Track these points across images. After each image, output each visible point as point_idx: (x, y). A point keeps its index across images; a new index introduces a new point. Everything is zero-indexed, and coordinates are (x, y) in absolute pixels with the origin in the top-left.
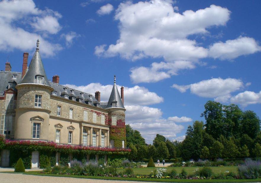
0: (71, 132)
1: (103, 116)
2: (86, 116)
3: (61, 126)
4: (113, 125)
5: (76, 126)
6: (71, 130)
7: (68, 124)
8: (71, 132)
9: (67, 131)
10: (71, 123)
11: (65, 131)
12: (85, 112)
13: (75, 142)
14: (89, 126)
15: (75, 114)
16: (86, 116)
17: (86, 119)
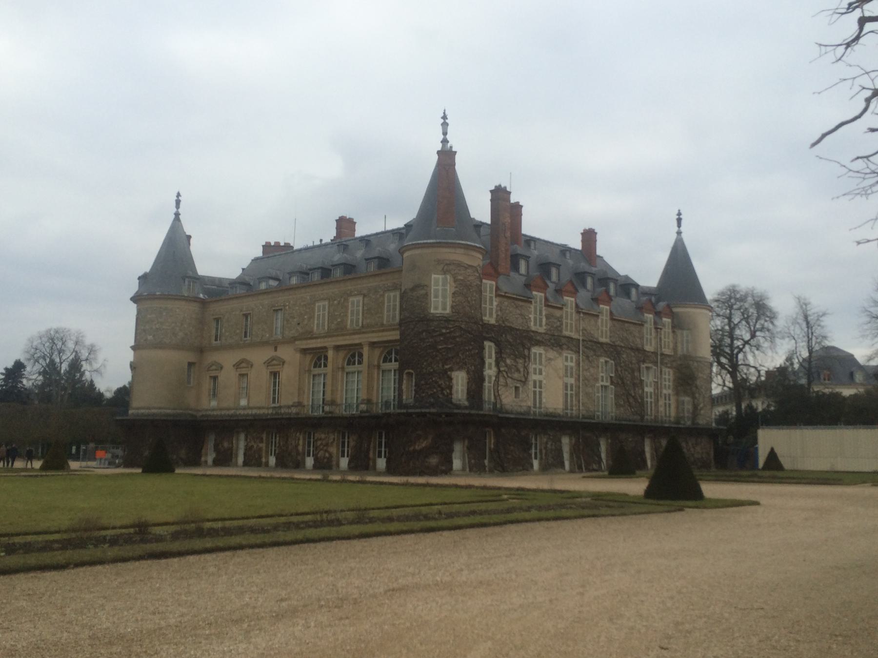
0: (275, 374)
1: (392, 294)
2: (324, 315)
3: (250, 365)
4: (432, 311)
5: (287, 353)
6: (276, 369)
7: (267, 353)
8: (275, 374)
9: (265, 374)
10: (276, 350)
11: (259, 376)
12: (319, 307)
13: (287, 399)
14: (319, 345)
15: (288, 321)
16: (324, 315)
17: (323, 325)
